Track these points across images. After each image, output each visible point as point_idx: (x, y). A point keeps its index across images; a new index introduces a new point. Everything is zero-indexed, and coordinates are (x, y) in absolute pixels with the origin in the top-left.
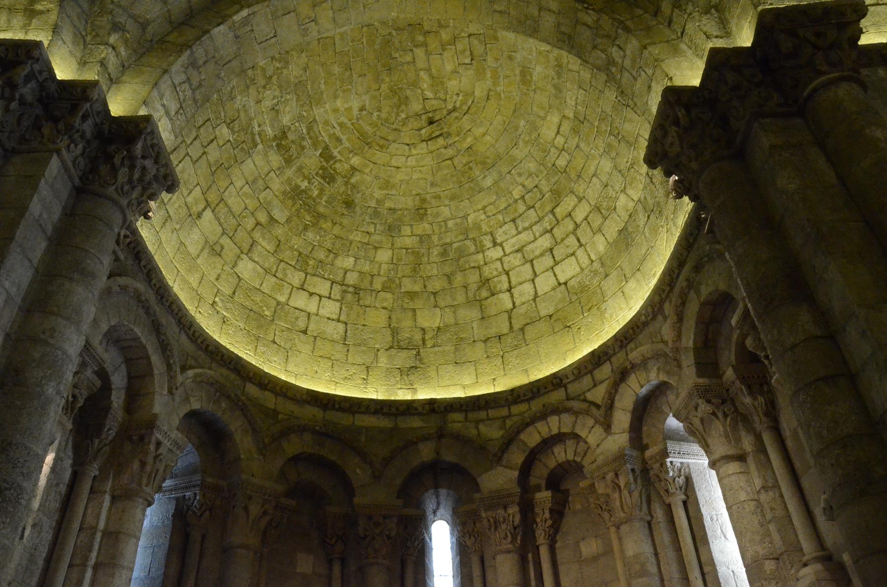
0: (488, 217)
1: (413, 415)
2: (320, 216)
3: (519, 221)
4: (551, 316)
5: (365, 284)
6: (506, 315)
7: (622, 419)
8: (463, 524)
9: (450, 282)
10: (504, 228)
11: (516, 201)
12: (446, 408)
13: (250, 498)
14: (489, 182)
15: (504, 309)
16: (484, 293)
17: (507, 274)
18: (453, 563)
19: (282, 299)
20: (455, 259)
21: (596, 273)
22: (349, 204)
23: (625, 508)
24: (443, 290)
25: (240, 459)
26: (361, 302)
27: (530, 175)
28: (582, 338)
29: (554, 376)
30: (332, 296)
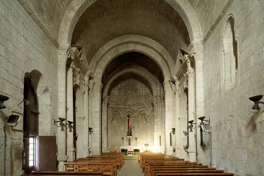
16: (136, 90)
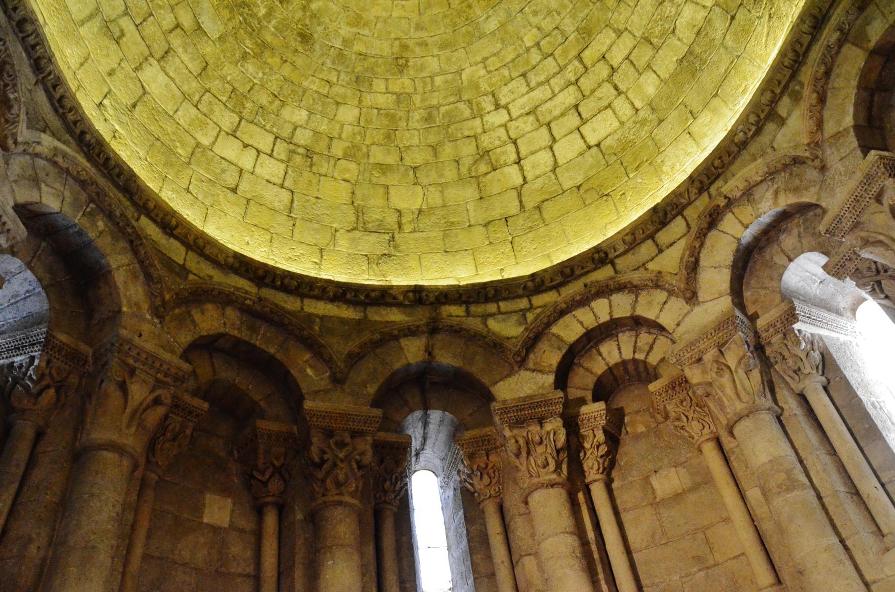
0: (489, 72)
1: (391, 305)
2: (264, 46)
3: (531, 76)
4: (578, 187)
5: (321, 147)
6: (514, 194)
7: (715, 278)
8: (471, 456)
9: (436, 155)
10: (510, 86)
11: (528, 50)
12: (437, 298)
13: (132, 372)
14: (492, 25)
15: (510, 185)
16: (483, 168)
17: (515, 142)
18: (448, 529)
19: (206, 141)
20: (442, 125)
21: (643, 122)
22: (305, 38)
23: (742, 394)
24: (427, 164)
25: (119, 311)
26: (314, 169)
27: (549, 13)
28: (628, 204)
29: (597, 249)
30: (275, 154)
